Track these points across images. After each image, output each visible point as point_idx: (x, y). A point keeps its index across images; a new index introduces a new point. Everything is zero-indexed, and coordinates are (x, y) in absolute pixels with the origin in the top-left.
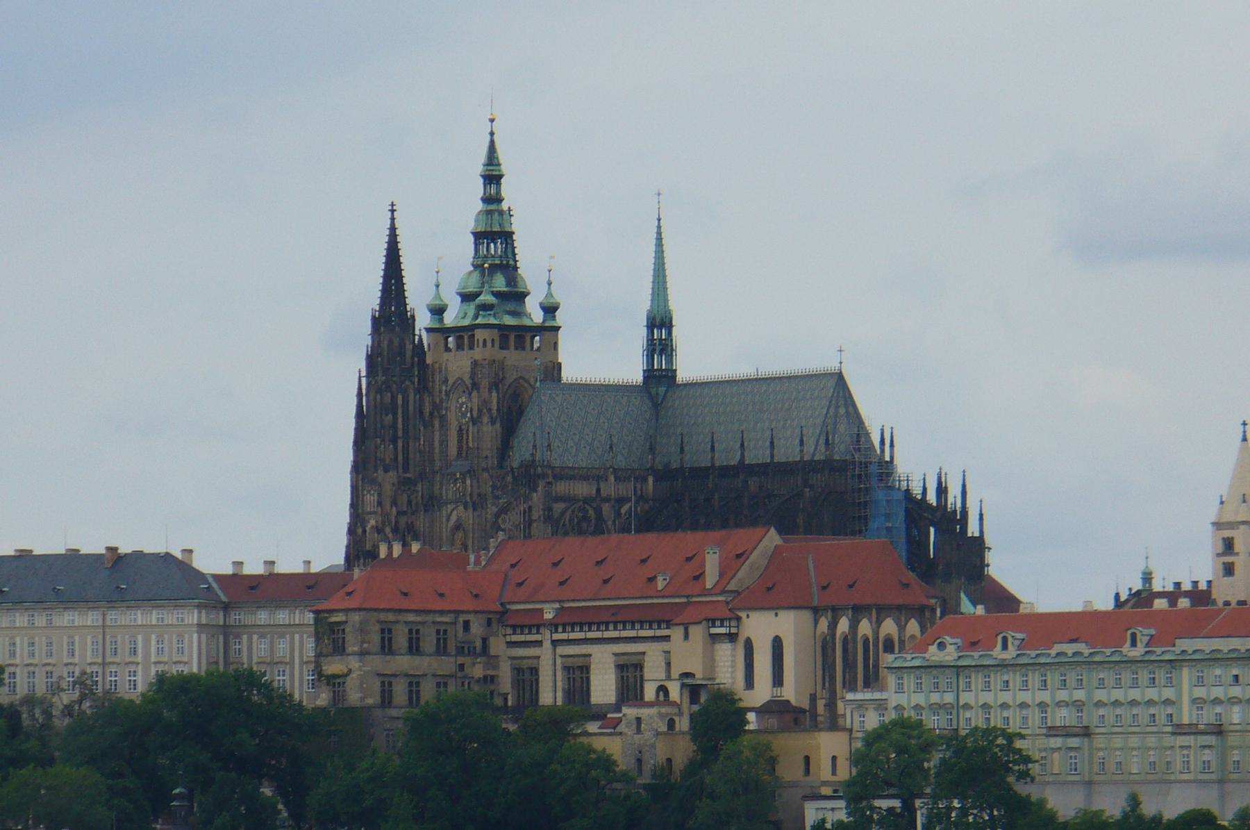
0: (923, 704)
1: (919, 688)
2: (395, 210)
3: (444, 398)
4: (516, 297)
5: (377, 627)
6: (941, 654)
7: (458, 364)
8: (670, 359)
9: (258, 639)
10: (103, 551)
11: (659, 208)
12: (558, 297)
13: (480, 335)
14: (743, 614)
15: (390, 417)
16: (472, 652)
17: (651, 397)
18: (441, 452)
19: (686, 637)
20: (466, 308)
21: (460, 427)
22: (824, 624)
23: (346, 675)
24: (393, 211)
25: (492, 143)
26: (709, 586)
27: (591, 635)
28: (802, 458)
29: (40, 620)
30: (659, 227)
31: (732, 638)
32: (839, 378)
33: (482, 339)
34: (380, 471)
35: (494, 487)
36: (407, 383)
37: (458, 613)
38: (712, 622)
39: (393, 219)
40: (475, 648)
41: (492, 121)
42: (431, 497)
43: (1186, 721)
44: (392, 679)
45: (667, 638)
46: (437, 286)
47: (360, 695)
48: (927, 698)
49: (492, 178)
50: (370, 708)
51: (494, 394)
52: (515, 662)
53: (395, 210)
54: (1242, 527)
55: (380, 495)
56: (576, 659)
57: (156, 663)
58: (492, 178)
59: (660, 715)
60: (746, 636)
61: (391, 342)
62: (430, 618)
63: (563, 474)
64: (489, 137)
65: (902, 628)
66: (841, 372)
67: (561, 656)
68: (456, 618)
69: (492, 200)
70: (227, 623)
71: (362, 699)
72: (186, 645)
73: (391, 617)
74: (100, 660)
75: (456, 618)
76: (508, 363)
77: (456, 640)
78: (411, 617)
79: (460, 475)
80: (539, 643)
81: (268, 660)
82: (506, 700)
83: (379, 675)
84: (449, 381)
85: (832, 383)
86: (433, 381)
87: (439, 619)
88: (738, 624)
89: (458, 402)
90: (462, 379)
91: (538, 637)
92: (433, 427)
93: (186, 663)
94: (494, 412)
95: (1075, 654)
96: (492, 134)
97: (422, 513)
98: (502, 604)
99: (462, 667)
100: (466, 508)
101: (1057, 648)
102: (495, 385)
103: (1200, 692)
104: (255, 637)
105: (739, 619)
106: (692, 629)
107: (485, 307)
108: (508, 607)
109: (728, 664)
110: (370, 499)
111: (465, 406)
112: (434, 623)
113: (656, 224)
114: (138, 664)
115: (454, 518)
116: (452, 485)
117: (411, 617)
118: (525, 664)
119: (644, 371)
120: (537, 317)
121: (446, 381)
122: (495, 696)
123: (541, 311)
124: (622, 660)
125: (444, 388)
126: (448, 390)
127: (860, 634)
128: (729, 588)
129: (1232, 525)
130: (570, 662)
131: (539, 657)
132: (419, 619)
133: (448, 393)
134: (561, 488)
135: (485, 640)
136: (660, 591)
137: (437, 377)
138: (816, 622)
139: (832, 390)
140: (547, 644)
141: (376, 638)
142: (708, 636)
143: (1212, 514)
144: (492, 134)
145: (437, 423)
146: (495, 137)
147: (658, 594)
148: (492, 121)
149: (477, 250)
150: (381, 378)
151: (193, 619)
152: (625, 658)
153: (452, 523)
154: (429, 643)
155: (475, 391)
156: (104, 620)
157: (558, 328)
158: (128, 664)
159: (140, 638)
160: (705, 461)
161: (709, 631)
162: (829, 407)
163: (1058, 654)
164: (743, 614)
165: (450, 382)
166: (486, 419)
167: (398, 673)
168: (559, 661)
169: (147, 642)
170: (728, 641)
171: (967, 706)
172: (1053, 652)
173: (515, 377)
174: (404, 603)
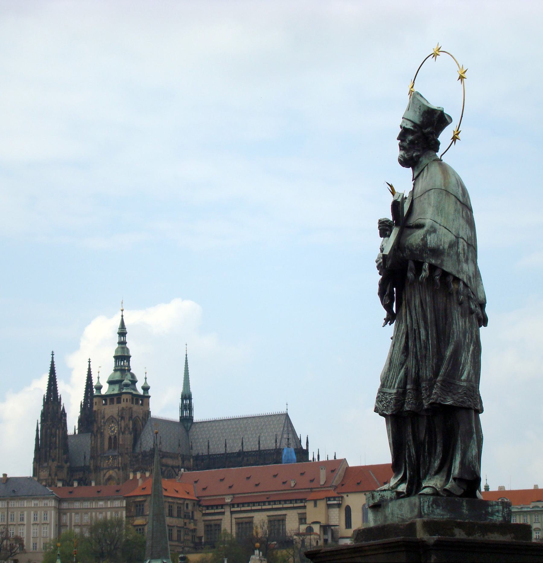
4: (134, 382)
7: (112, 410)
9: (75, 515)
11: (186, 350)
12: (149, 384)
13: (124, 397)
14: (345, 496)
16: (189, 518)
17: (185, 427)
19: (315, 505)
21: (110, 438)
23: (145, 525)
26: (322, 483)
27: (254, 508)
28: (276, 447)
30: (186, 358)
31: (339, 506)
32: (287, 415)
33: (126, 398)
36: (60, 425)
37: (185, 499)
38: (329, 499)
40: (190, 516)
45: (305, 507)
51: (131, 422)
55: (50, 471)
56: (244, 519)
57: (33, 524)
59: (314, 539)
61: (53, 408)
62: (176, 501)
63: (164, 455)
64: (121, 317)
66: (287, 413)
67: (236, 518)
69: (123, 343)
70: (60, 508)
72: (48, 516)
78: (170, 500)
80: (223, 513)
81: (80, 524)
85: (283, 418)
86: (98, 417)
87: (179, 502)
88: (342, 500)
89: (109, 426)
91: (223, 510)
92: (97, 436)
93: (48, 524)
96: (122, 316)
97: (94, 472)
98: (197, 497)
101: (532, 505)
102: (131, 418)
104: (73, 514)
105: (342, 497)
106: (318, 502)
107: (127, 385)
108: (200, 498)
109: (337, 517)
110: (44, 474)
111: (114, 428)
112: (177, 503)
113: (185, 357)
114: (24, 525)
115: (107, 475)
116: (107, 461)
117: (170, 500)
118: (213, 523)
120: (141, 392)
121: (104, 417)
122: (196, 538)
124: (272, 518)
125: (103, 421)
130: (240, 521)
131: (221, 520)
133: (105, 423)
134: (164, 461)
135: (193, 512)
137: (99, 416)
139: (284, 420)
140: (228, 513)
142: (326, 504)
144: (122, 316)
145: (99, 436)
146: (123, 317)
147: (291, 489)
149: (116, 364)
150: (49, 423)
151: (52, 504)
152: (275, 517)
154: (175, 513)
155: (123, 421)
156: (8, 505)
157: (149, 397)
158: (19, 525)
159: (25, 513)
160: (222, 451)
163: (533, 507)
164: (345, 496)
165: (106, 418)
166: (127, 433)
169: (29, 515)
170: (337, 507)
172: (531, 506)
173: (135, 416)
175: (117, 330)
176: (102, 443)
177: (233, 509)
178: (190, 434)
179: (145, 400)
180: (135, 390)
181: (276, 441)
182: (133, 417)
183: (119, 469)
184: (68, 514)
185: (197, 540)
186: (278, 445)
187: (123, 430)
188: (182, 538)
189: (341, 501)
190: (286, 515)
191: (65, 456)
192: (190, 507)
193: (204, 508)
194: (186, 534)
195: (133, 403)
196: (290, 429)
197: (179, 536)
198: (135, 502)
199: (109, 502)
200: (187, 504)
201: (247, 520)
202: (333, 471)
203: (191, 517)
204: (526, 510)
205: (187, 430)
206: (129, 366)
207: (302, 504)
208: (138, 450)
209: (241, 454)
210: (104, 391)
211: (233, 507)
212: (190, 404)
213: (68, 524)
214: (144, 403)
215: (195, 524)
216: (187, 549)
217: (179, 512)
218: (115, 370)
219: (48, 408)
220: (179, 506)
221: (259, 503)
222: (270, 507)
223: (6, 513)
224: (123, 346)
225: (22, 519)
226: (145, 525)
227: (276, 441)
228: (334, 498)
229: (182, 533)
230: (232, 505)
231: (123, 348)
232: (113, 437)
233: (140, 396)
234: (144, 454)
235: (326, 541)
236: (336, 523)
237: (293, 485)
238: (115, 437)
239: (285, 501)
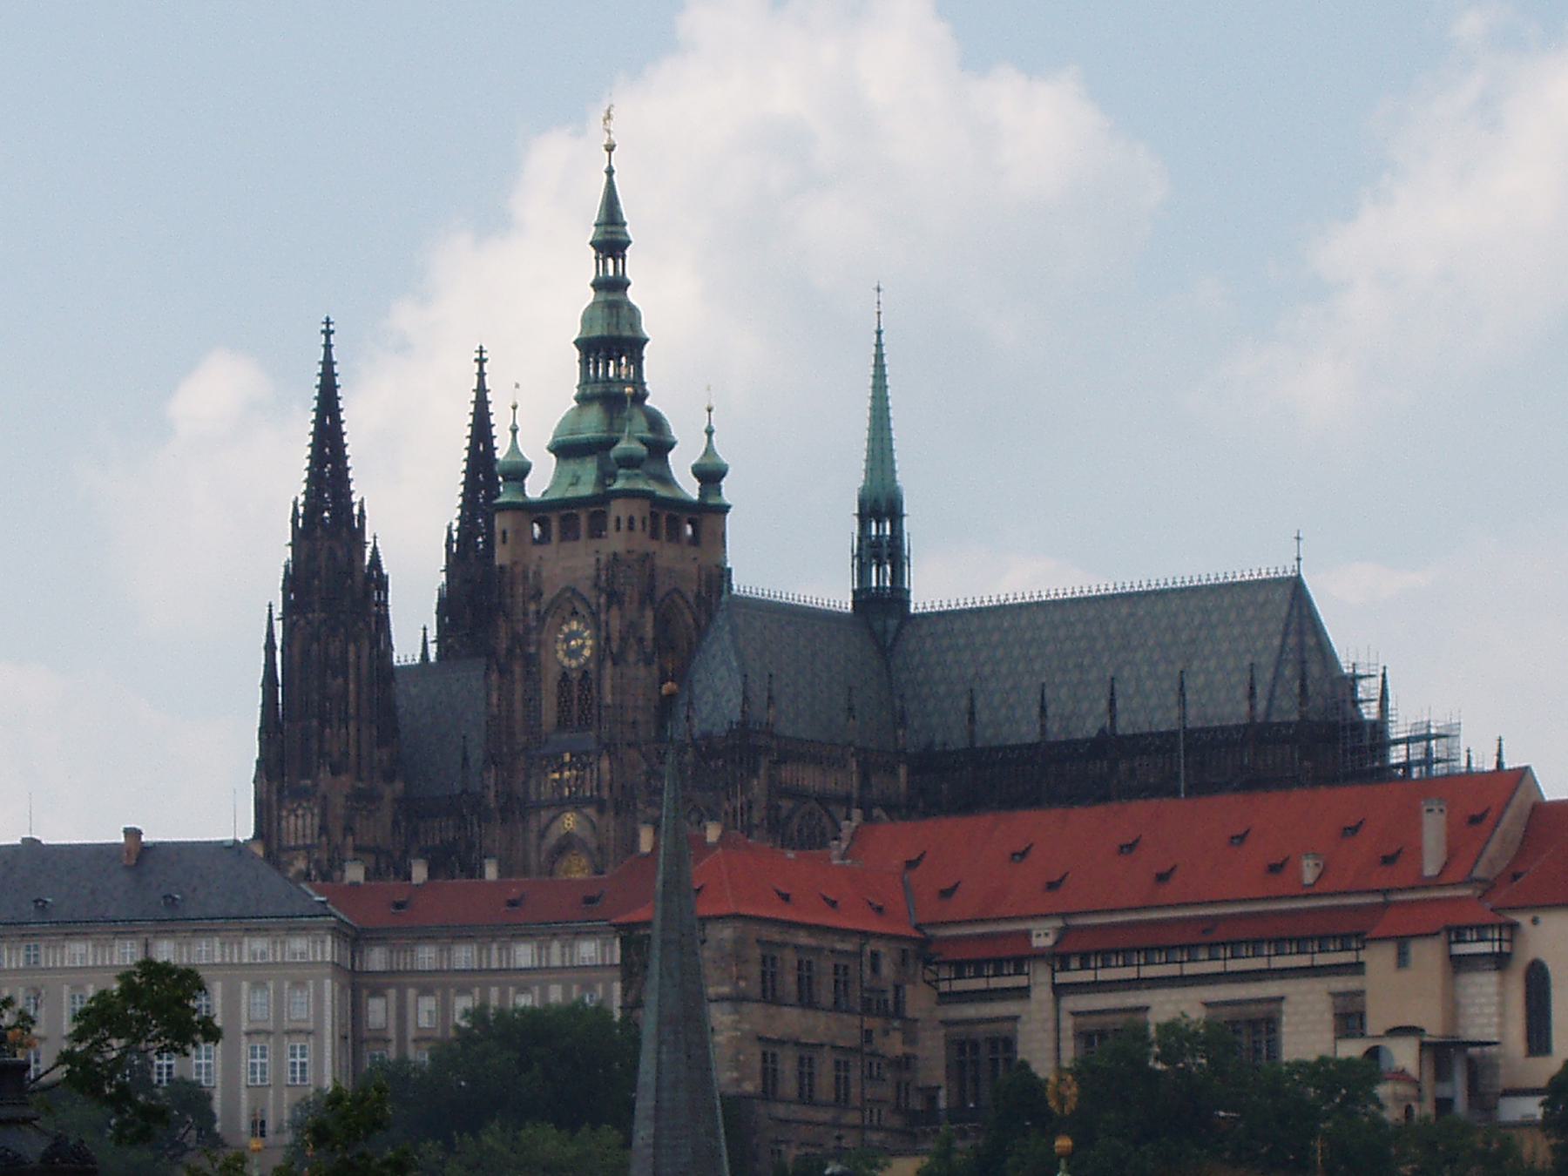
2: (333, 332)
3: (534, 624)
4: (660, 446)
5: (756, 953)
8: (898, 575)
11: (879, 313)
12: (724, 453)
13: (618, 509)
14: (1523, 919)
15: (340, 680)
19: (1402, 960)
20: (576, 467)
24: (328, 333)
25: (610, 186)
26: (1431, 869)
28: (1252, 718)
30: (879, 345)
31: (1500, 962)
32: (1296, 587)
34: (324, 775)
36: (361, 625)
37: (865, 935)
38: (1457, 933)
39: (328, 347)
41: (610, 148)
44: (777, 1050)
45: (1357, 968)
47: (735, 1075)
50: (747, 1097)
51: (649, 614)
52: (956, 1029)
53: (333, 332)
55: (324, 815)
56: (1109, 1019)
60: (1529, 958)
63: (792, 752)
66: (1299, 575)
67: (1075, 1014)
68: (862, 945)
69: (611, 288)
71: (738, 1081)
73: (775, 935)
75: (862, 945)
76: (658, 562)
77: (861, 986)
78: (803, 939)
79: (572, 756)
80: (1023, 993)
83: (760, 1039)
84: (545, 596)
85: (1281, 596)
87: (839, 946)
90: (573, 591)
91: (1021, 981)
93: (309, 1033)
94: (649, 643)
96: (610, 172)
98: (918, 927)
99: (868, 1035)
102: (648, 596)
104: (411, 993)
105: (1514, 927)
107: (629, 462)
108: (929, 932)
109: (1493, 1009)
110: (299, 825)
113: (875, 340)
117: (803, 939)
119: (854, 592)
120: (690, 488)
121: (538, 595)
123: (695, 480)
126: (543, 610)
128: (1479, 873)
130: (1093, 1023)
132: (812, 942)
134: (787, 773)
135: (898, 988)
136: (1309, 885)
140: (1042, 993)
141: (755, 971)
144: (610, 172)
145: (518, 670)
146: (615, 177)
148: (610, 148)
150: (316, 616)
151: (323, 953)
152: (1236, 1009)
153: (552, 839)
154: (826, 995)
155: (615, 611)
157: (725, 509)
160: (1027, 732)
161: (1450, 949)
162: (1285, 634)
164: (1523, 919)
165: (547, 596)
166: (631, 658)
167: (786, 1039)
170: (1494, 966)
174: (788, 914)
176: (532, 701)
179: (708, 522)
180: (666, 479)
182: (660, 593)
183: (601, 807)
184: (392, 993)
185: (917, 1103)
186: (1261, 706)
187: (615, 646)
188: (855, 1091)
189: (1510, 941)
190: (1282, 999)
192: (887, 969)
193: (945, 973)
195: (654, 535)
197: (841, 1083)
199: (556, 947)
200: (875, 955)
201: (1120, 1020)
202: (1475, 820)
203: (891, 1008)
205: (885, 648)
206: (638, 381)
208: (677, 730)
209: (1107, 744)
210: (536, 487)
211: (1065, 968)
213: (392, 1034)
215: (910, 1038)
216: (875, 1137)
218: (583, 399)
220: (843, 961)
228: (1481, 931)
229: (855, 1075)
230: (1058, 958)
233: (683, 505)
234: (705, 748)
235: (1444, 1105)
236: (1490, 1034)
237: (1309, 875)
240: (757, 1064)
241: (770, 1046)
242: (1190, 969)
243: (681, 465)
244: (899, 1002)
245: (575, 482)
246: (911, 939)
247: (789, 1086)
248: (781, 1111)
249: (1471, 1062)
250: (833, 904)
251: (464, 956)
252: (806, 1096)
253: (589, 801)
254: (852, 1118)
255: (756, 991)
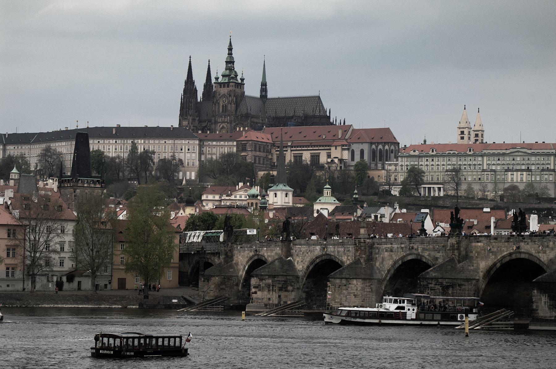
0: (409, 164)
1: (407, 161)
4: (236, 76)
5: (254, 145)
6: (414, 153)
10: (170, 127)
12: (244, 77)
13: (231, 84)
14: (351, 144)
17: (263, 101)
18: (218, 111)
19: (336, 149)
21: (223, 106)
22: (374, 146)
23: (247, 156)
24: (190, 58)
25: (230, 41)
29: (157, 142)
30: (264, 63)
31: (348, 149)
32: (319, 97)
34: (189, 117)
35: (234, 119)
38: (343, 145)
39: (190, 59)
41: (230, 36)
42: (215, 121)
43: (485, 168)
46: (217, 73)
48: (410, 163)
49: (230, 49)
51: (235, 98)
54: (467, 128)
55: (188, 122)
58: (230, 49)
59: (335, 166)
63: (253, 117)
65: (395, 148)
67: (293, 154)
69: (230, 54)
73: (256, 143)
74: (173, 151)
76: (236, 91)
80: (287, 151)
82: (274, 164)
91: (287, 149)
95: (453, 153)
96: (230, 39)
99: (267, 155)
100: (228, 123)
102: (234, 96)
103: (489, 162)
104: (207, 148)
106: (337, 147)
107: (233, 78)
110: (185, 123)
115: (221, 126)
117: (260, 143)
120: (240, 81)
124: (313, 154)
127: (385, 149)
128: (346, 138)
129: (463, 128)
134: (252, 119)
135: (270, 149)
138: (371, 146)
140: (289, 151)
141: (254, 147)
143: (458, 125)
144: (230, 39)
145: (217, 104)
154: (262, 150)
155: (230, 98)
157: (244, 84)
159: (183, 146)
160: (283, 115)
163: (448, 153)
164: (351, 144)
165: (221, 95)
168: (292, 155)
169: (185, 148)
171: (422, 165)
172: (447, 153)
174: (258, 140)
175: (227, 47)
176: (219, 108)
177: (292, 149)
178: (266, 105)
179: (242, 86)
180: (237, 80)
181: (313, 111)
182: (236, 95)
183: (228, 123)
184: (205, 148)
185: (272, 164)
187: (230, 102)
188: (265, 162)
190: (320, 153)
191: (196, 114)
194: (267, 161)
195: (235, 88)
196: (321, 105)
197: (263, 162)
198: (241, 143)
199: (226, 142)
200: (268, 145)
201: (299, 155)
202: (345, 131)
204: (444, 155)
205: (264, 103)
206: (234, 67)
207: (329, 148)
208: (238, 113)
210: (220, 80)
211: (292, 148)
212: (266, 88)
213: (205, 153)
214: (242, 87)
215: (272, 156)
217: (264, 149)
218: (226, 69)
219: (188, 87)
221: (306, 146)
222: (312, 148)
223: (173, 146)
224: (231, 56)
225: (182, 150)
226: (247, 156)
227: (313, 111)
228: (346, 145)
229: (265, 160)
231: (230, 57)
232: (225, 105)
233: (239, 83)
234: (242, 115)
235: (341, 167)
236: (347, 158)
238: (226, 105)
239: (320, 146)
240: (254, 159)
241: (255, 157)
242: (308, 148)
243: (239, 78)
244: (271, 151)
245: (225, 80)
246: (272, 143)
247: (257, 162)
248: (256, 165)
249: (344, 161)
250: (263, 139)
251: (214, 143)
252: (259, 163)
253: (226, 122)
254: (265, 166)
255: (254, 150)
